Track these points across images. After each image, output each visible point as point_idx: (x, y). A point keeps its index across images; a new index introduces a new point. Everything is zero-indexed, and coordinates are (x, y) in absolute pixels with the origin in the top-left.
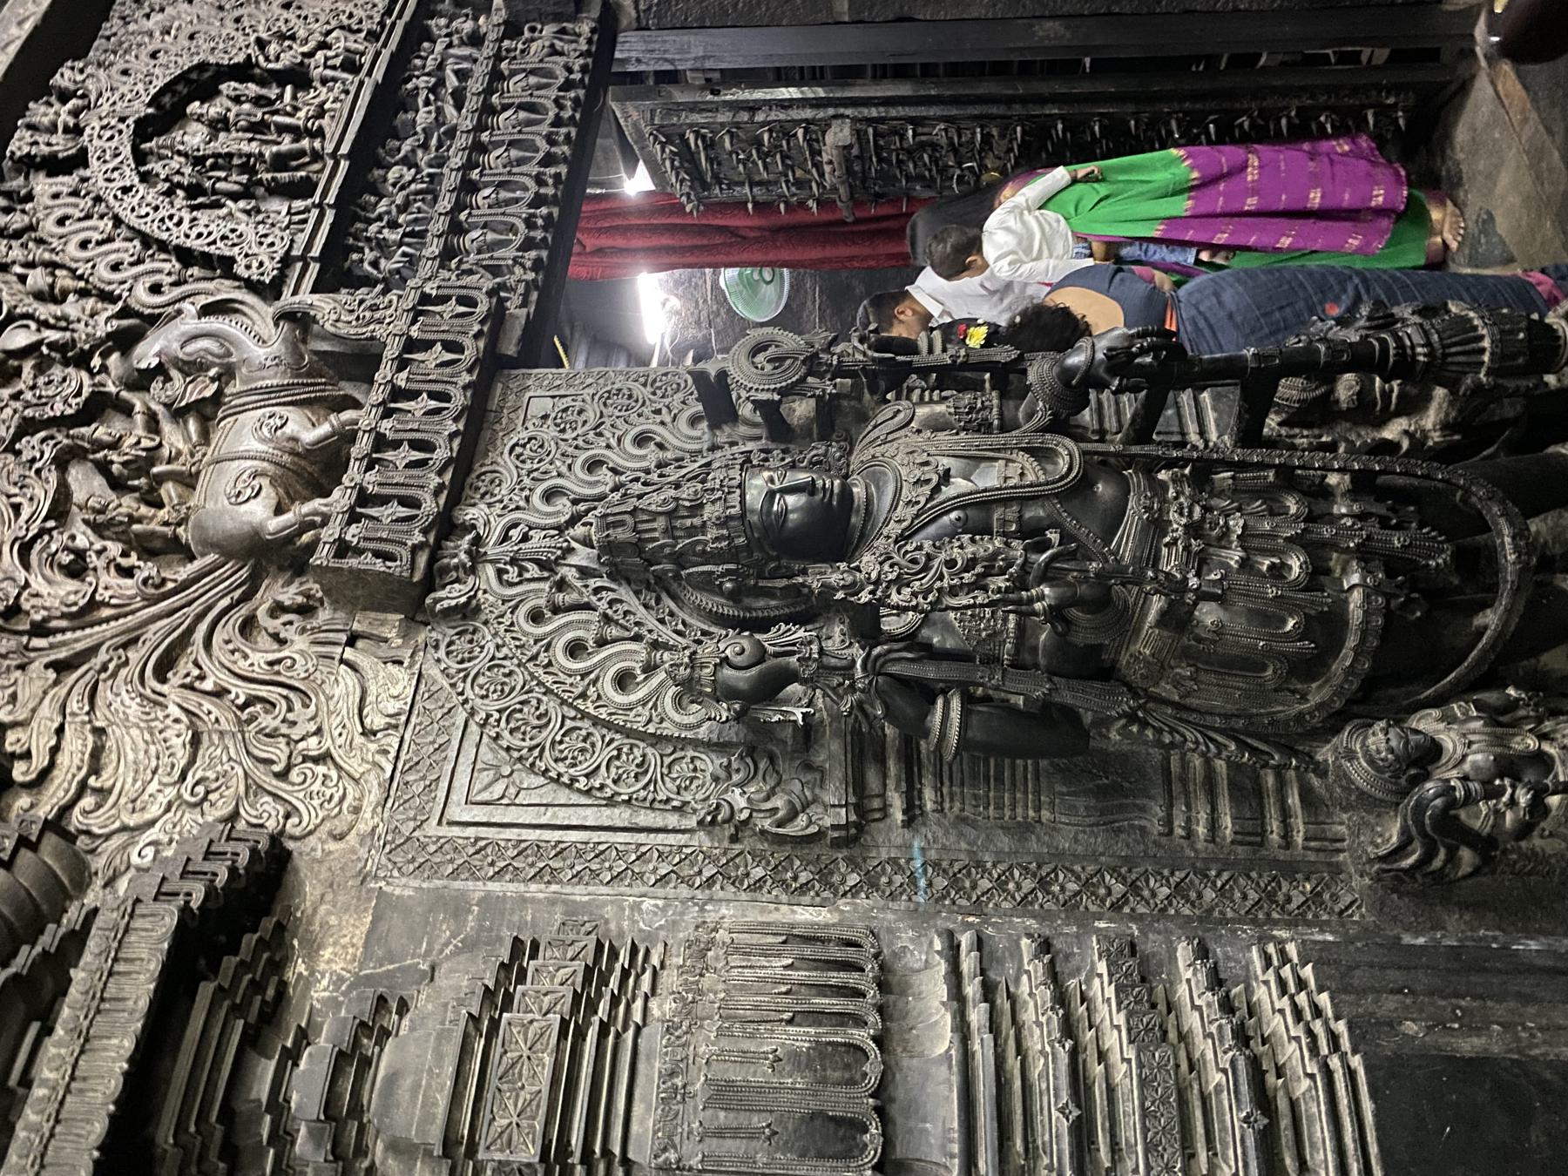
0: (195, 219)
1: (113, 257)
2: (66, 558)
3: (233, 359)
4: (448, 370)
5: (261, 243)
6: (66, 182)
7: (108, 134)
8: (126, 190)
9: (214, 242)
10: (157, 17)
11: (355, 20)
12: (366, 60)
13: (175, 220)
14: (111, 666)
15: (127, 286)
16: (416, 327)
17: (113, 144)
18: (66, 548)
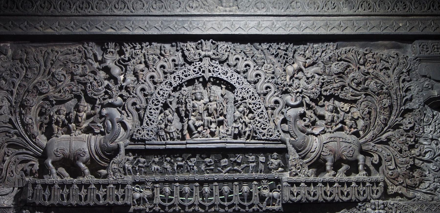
0: (157, 109)
1: (147, 88)
2: (43, 110)
3: (107, 134)
4: (95, 198)
5: (149, 131)
6: (181, 61)
7: (197, 70)
8: (171, 84)
9: (148, 117)
10: (272, 57)
11: (261, 130)
12: (242, 140)
13: (157, 103)
14: (10, 134)
15: (135, 95)
16: (112, 186)
17: (191, 72)
18: (46, 110)
